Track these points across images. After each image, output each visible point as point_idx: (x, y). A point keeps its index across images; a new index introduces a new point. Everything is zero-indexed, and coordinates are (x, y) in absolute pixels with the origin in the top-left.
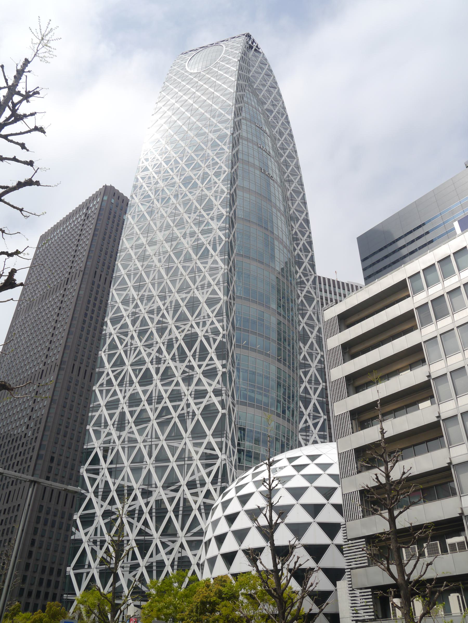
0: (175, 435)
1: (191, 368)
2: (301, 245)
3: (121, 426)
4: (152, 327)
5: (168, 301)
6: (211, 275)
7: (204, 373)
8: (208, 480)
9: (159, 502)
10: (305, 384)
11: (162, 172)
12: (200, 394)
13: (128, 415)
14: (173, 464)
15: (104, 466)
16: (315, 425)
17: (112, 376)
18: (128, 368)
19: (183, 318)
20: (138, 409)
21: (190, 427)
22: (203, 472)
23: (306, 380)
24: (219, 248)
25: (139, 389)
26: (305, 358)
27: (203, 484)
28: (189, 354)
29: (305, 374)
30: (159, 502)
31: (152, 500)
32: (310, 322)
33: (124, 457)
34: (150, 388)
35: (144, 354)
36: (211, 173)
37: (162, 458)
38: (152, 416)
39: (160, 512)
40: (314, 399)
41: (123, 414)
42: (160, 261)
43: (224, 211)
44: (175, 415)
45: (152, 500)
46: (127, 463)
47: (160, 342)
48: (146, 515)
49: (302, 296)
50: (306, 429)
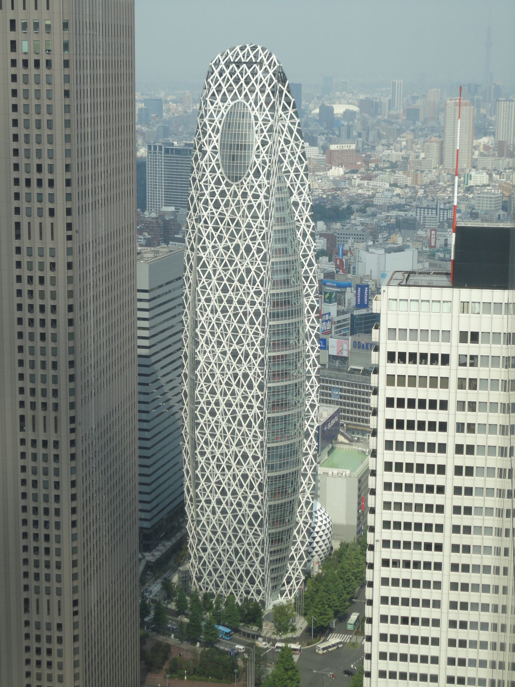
0: (240, 522)
1: (246, 492)
2: (311, 362)
3: (214, 512)
4: (224, 465)
5: (231, 450)
6: (254, 440)
7: (253, 497)
8: (256, 544)
9: (236, 549)
10: (306, 465)
11: (216, 336)
12: (251, 507)
13: (217, 509)
14: (240, 534)
15: (209, 529)
16: (308, 489)
17: (205, 486)
18: (213, 484)
19: (239, 463)
20: (222, 507)
21: (248, 521)
22: (254, 540)
23: (306, 463)
24: (258, 423)
25: (221, 497)
26: (306, 449)
27: (254, 545)
28: (245, 485)
29: (306, 459)
30: (236, 549)
31: (233, 547)
32: (312, 424)
33: (217, 527)
34: (227, 498)
35: (221, 479)
36: (251, 354)
37: (235, 530)
38: (229, 512)
39: (236, 552)
40: (309, 473)
41: (214, 508)
42: (223, 420)
43: (260, 393)
44: (240, 514)
45: (233, 547)
46: (219, 531)
47: (229, 474)
48: (230, 552)
49: (308, 405)
50: (304, 491)
